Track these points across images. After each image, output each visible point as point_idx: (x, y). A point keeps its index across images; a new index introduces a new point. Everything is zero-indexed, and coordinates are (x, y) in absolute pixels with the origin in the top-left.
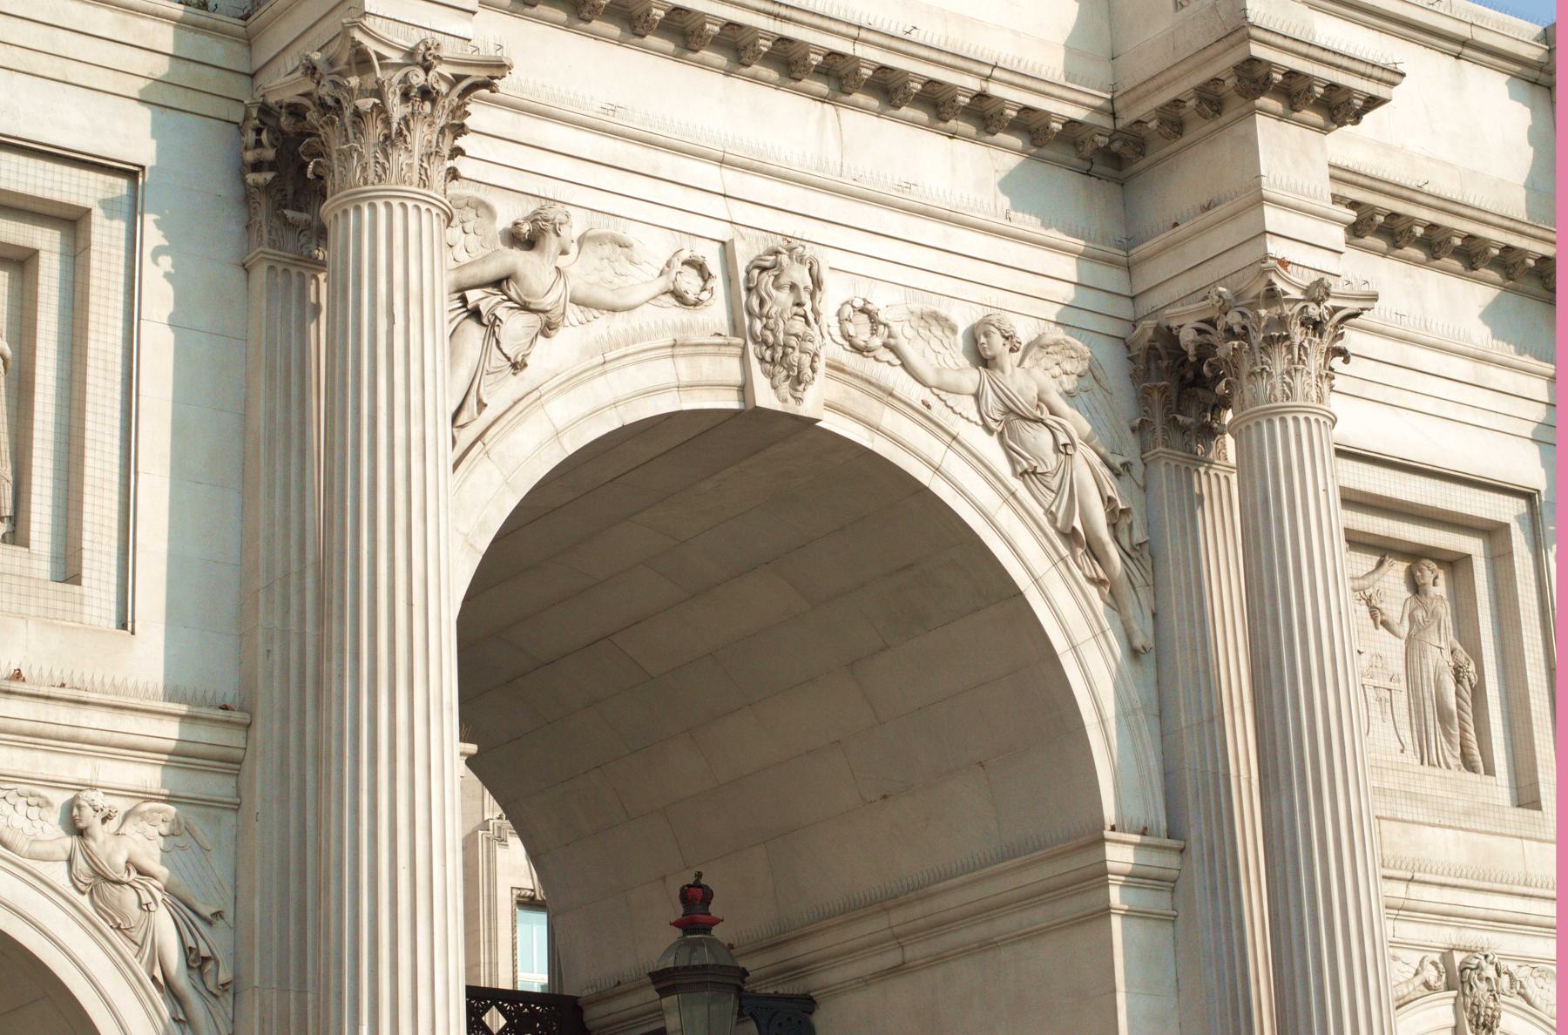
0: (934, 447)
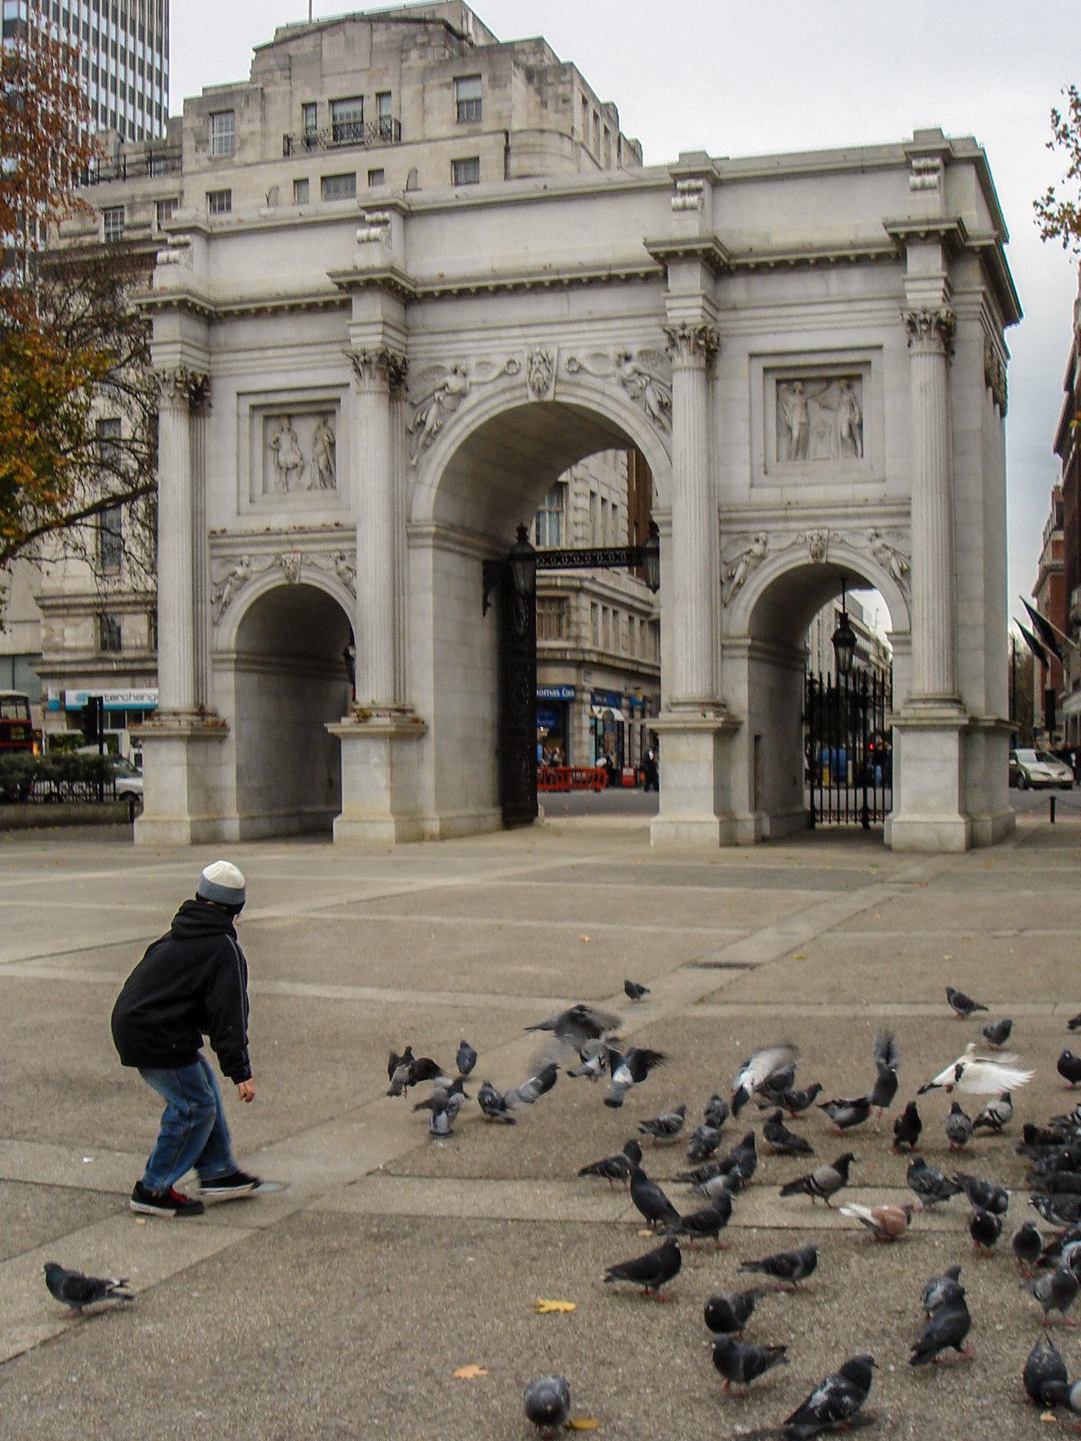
0: (598, 398)
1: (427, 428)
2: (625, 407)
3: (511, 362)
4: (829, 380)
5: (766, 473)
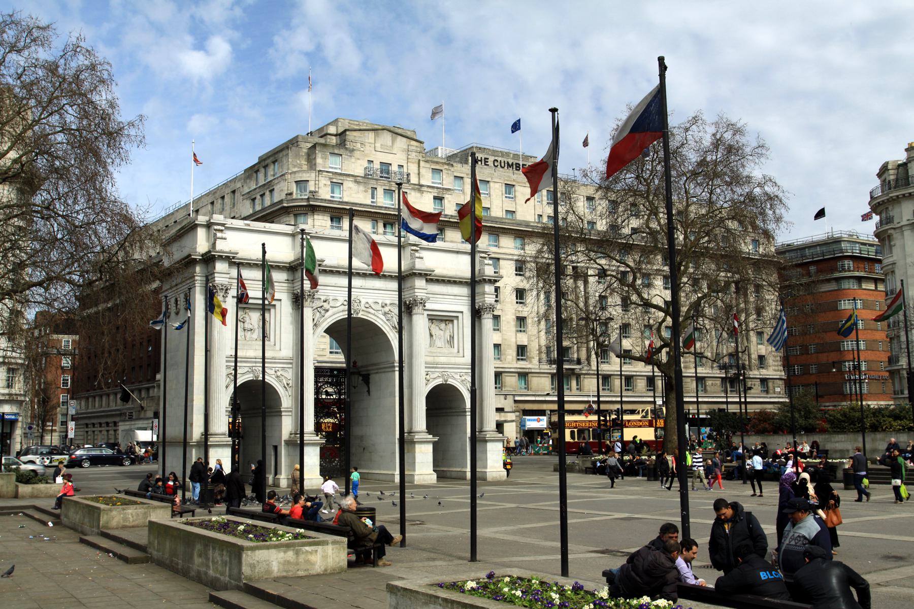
4: (442, 320)
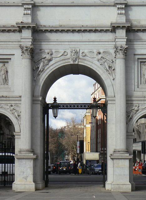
1: (39, 70)
2: (99, 67)
3: (64, 52)
5: (138, 87)
